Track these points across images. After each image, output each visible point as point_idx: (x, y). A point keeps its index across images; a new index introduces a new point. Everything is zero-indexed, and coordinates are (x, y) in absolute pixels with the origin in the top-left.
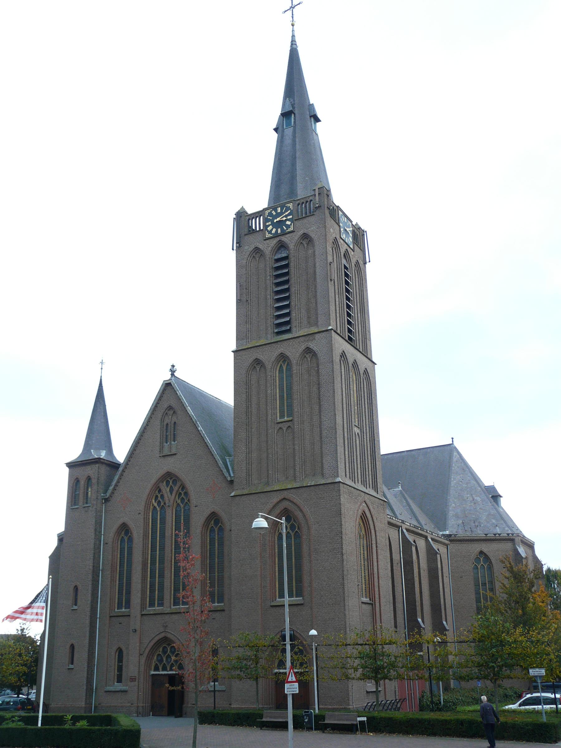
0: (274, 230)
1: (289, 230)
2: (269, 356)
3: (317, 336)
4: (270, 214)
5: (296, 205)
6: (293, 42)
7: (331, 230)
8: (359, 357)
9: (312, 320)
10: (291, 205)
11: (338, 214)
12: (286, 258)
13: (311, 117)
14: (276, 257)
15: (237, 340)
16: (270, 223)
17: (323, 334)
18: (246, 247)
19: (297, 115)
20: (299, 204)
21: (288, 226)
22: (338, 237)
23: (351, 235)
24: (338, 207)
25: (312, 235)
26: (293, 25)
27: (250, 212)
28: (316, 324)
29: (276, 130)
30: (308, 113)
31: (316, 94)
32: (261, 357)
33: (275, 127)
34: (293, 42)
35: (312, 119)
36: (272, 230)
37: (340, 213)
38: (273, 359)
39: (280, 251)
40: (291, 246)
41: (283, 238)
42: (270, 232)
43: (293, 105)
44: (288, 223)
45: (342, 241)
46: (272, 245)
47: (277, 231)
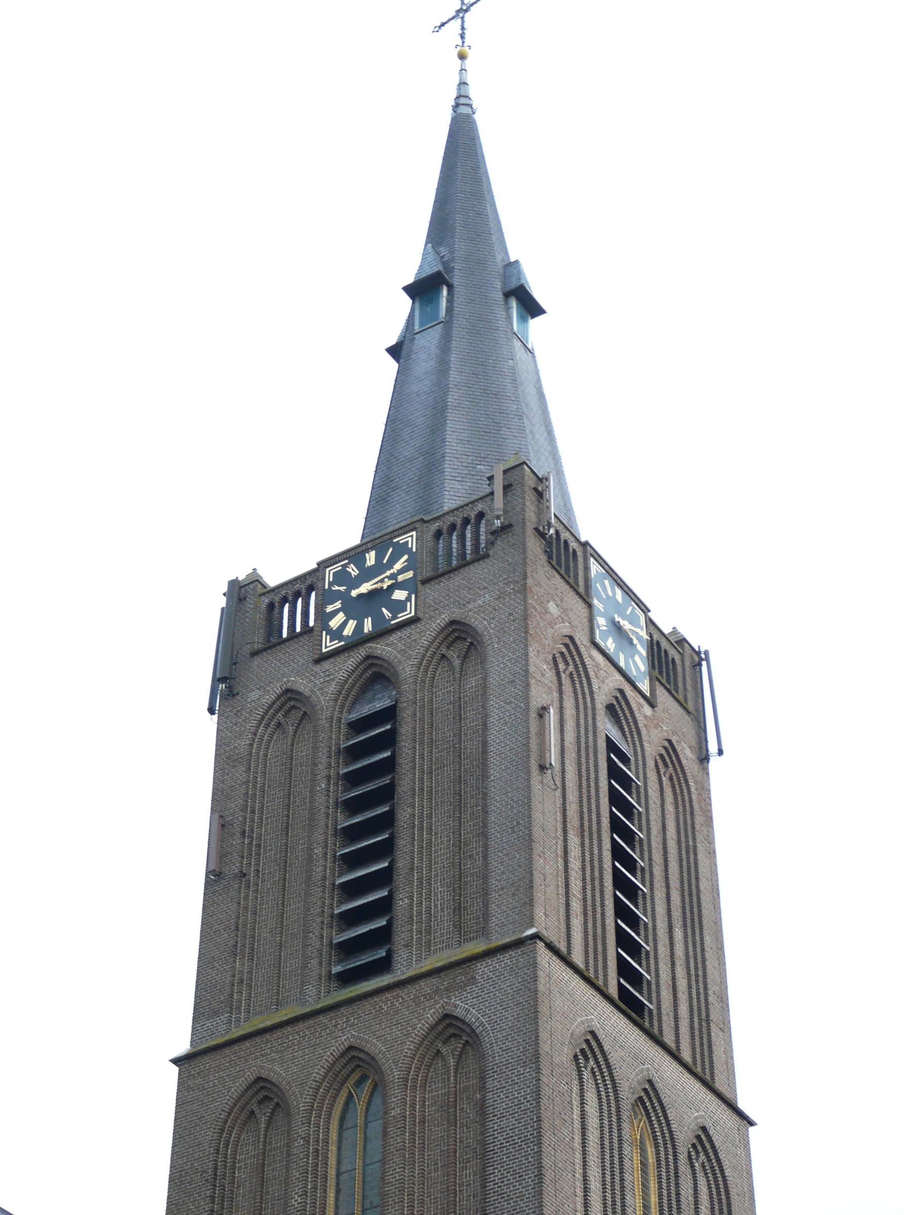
0: (352, 625)
1: (402, 617)
2: (299, 1065)
3: (482, 969)
4: (342, 577)
5: (429, 536)
6: (462, 100)
7: (552, 607)
8: (673, 1080)
9: (468, 914)
10: (410, 539)
11: (587, 569)
12: (390, 714)
13: (507, 295)
14: (354, 716)
15: (195, 1019)
16: (338, 605)
17: (505, 959)
18: (254, 695)
19: (458, 289)
20: (438, 534)
21: (400, 606)
22: (582, 639)
23: (644, 653)
24: (585, 545)
25: (479, 623)
26: (462, 57)
27: (272, 581)
28: (484, 931)
29: (395, 351)
30: (498, 284)
31: (528, 234)
32: (276, 1071)
33: (393, 341)
34: (462, 100)
35: (514, 303)
36: (344, 625)
37: (595, 568)
38: (318, 1073)
39: (369, 695)
40: (406, 670)
41: (380, 648)
42: (336, 634)
43: (445, 264)
44: (399, 595)
45: (599, 658)
46: (341, 675)
47: (359, 627)
